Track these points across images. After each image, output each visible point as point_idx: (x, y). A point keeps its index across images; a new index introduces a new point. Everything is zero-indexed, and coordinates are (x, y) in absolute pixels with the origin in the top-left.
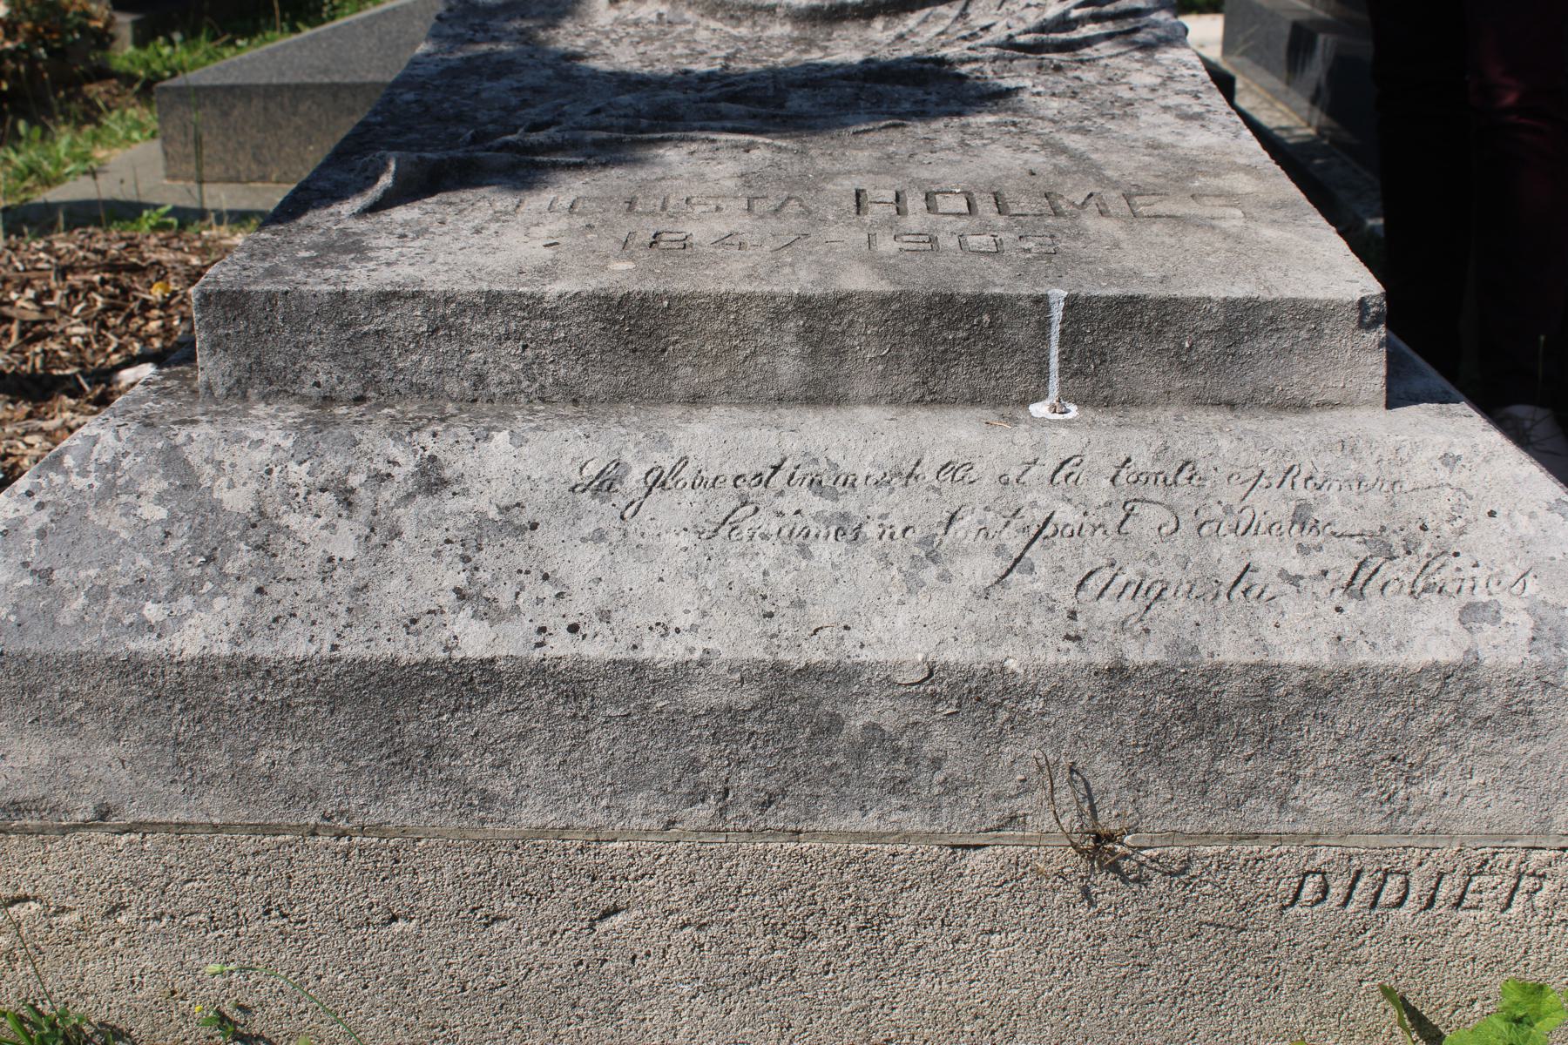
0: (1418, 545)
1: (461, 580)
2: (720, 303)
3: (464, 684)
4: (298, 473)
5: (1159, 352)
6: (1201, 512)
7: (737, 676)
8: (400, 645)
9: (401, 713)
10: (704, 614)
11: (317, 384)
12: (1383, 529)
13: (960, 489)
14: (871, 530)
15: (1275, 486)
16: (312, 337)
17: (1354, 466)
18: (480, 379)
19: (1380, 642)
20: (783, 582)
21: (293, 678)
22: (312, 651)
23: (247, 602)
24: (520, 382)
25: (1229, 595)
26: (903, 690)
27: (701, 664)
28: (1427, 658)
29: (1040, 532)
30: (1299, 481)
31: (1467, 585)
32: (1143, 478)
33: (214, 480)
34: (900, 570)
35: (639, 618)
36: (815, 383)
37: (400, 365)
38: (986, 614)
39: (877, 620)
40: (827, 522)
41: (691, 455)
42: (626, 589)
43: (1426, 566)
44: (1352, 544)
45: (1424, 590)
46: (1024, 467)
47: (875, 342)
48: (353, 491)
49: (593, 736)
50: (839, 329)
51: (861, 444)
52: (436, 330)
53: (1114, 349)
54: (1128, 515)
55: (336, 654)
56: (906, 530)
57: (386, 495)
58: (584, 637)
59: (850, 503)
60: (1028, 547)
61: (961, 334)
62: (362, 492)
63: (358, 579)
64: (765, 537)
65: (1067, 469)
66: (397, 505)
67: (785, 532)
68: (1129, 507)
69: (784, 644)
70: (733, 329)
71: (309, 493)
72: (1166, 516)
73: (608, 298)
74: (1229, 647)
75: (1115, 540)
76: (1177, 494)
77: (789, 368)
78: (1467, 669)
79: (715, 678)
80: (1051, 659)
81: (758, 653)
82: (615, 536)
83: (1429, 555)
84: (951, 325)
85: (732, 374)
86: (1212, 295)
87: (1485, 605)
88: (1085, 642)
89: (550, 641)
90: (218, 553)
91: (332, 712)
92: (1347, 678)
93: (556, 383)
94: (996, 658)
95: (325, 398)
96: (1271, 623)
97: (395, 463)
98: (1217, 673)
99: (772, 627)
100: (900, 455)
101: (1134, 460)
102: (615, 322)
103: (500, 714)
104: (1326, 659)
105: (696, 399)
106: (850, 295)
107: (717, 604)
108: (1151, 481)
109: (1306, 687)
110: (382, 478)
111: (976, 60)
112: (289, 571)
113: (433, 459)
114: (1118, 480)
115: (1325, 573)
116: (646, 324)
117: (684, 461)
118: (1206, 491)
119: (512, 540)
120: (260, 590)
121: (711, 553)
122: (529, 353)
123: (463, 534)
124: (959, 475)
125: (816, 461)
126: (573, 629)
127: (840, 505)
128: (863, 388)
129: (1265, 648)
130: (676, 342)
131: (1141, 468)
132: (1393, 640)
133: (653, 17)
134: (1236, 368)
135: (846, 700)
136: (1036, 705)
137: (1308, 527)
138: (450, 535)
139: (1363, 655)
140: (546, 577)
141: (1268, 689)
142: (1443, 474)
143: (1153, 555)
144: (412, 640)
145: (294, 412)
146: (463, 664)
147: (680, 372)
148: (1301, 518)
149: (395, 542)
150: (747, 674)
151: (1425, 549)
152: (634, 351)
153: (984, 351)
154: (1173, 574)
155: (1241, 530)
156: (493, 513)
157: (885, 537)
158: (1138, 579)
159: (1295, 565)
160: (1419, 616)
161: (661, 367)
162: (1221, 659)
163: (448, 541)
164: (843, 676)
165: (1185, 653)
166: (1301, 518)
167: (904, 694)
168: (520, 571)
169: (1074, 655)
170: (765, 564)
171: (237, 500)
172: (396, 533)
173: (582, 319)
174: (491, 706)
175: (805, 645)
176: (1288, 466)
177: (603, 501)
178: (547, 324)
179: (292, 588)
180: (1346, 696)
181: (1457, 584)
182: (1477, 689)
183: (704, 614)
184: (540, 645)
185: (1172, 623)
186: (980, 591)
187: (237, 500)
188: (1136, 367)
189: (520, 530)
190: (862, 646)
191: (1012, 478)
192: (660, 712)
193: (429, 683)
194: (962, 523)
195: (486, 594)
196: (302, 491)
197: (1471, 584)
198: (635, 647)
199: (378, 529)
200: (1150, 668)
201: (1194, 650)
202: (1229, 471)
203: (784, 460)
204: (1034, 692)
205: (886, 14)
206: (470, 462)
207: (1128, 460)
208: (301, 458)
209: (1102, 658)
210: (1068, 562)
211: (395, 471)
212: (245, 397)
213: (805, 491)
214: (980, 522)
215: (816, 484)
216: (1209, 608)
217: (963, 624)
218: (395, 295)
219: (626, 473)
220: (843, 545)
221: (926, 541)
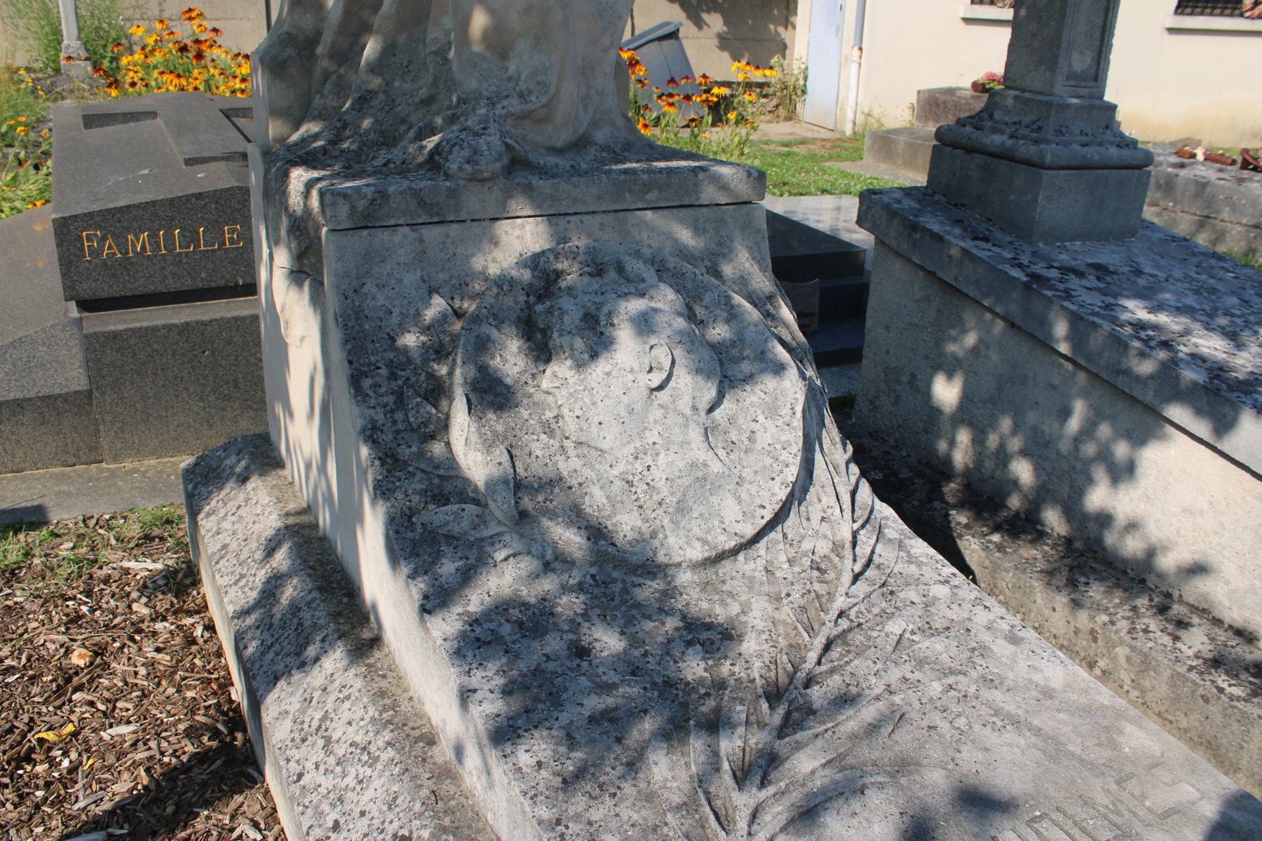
133: (589, 579)
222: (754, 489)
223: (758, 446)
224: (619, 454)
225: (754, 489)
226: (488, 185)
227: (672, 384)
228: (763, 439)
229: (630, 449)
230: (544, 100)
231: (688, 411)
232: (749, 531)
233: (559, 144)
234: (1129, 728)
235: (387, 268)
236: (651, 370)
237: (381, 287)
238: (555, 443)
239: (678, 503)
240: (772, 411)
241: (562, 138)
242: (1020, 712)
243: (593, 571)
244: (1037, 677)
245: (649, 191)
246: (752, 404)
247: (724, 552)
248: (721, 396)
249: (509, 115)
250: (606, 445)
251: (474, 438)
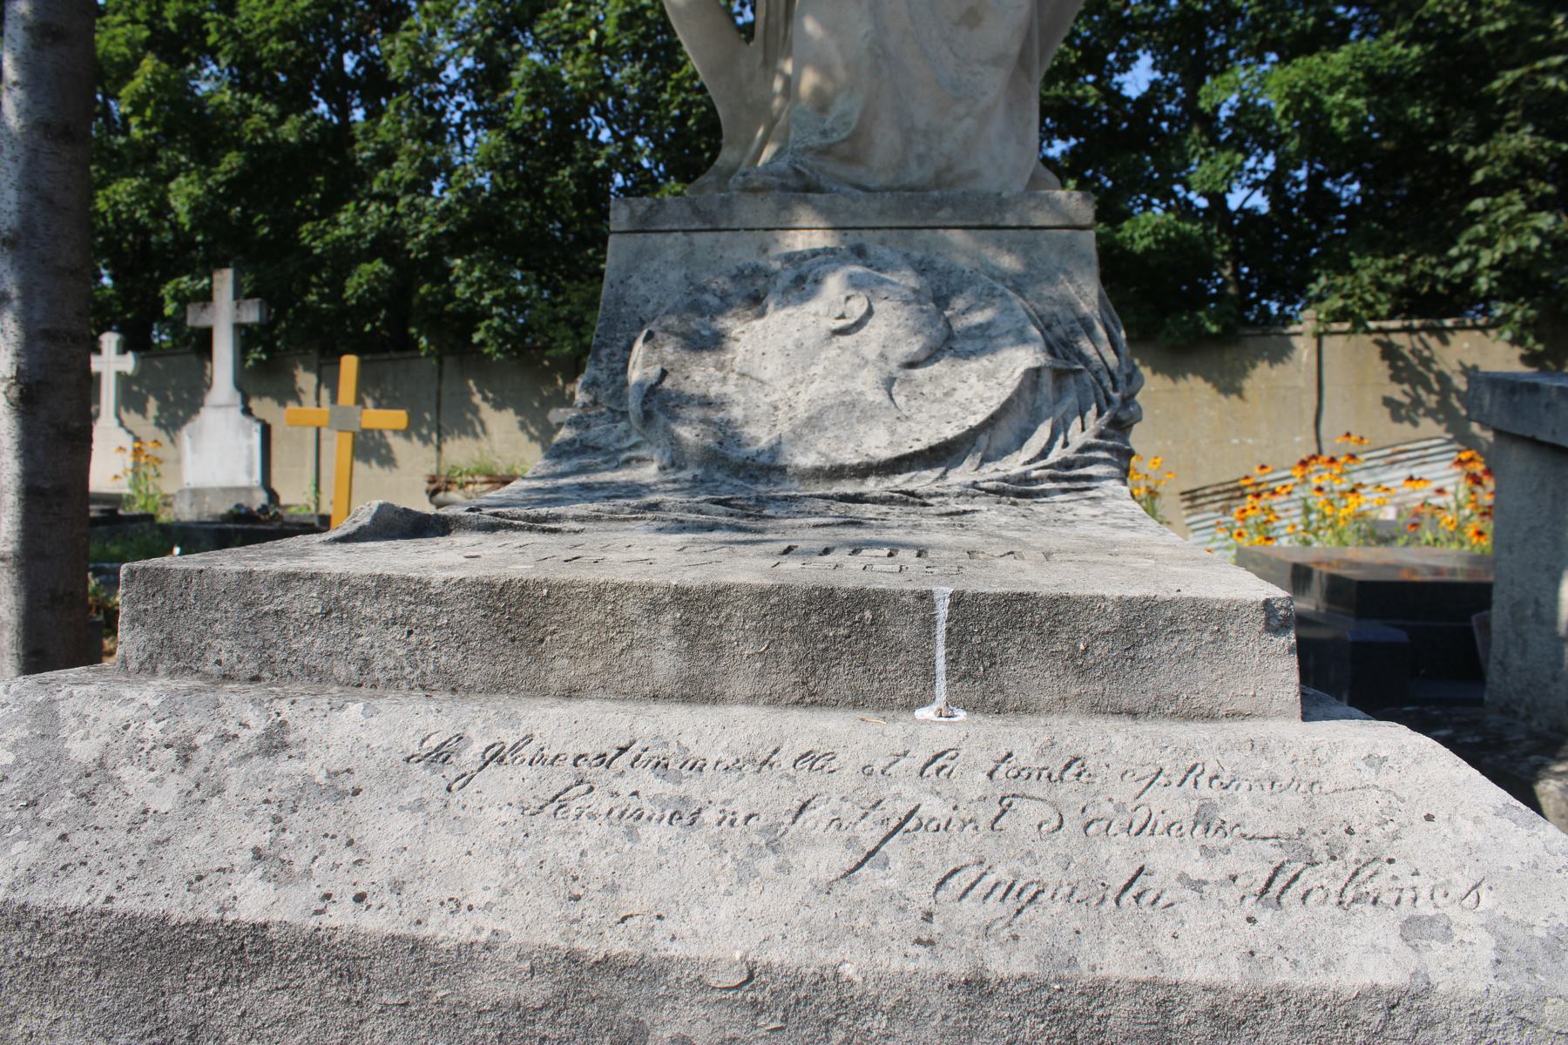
0: (1345, 849)
1: (261, 838)
2: (598, 593)
3: (234, 952)
5: (1053, 654)
6: (1088, 810)
7: (527, 965)
8: (175, 902)
9: (167, 982)
10: (504, 892)
11: (219, 662)
12: (1302, 832)
13: (816, 778)
14: (710, 816)
15: (1175, 784)
16: (218, 615)
17: (1265, 765)
18: (366, 662)
19: (1303, 959)
20: (600, 864)
21: (62, 932)
22: (85, 902)
23: (45, 848)
24: (402, 668)
25: (1117, 901)
26: (717, 995)
27: (488, 948)
28: (1364, 980)
29: (901, 825)
30: (1203, 780)
31: (1407, 896)
32: (1025, 774)
33: (72, 731)
34: (733, 858)
35: (433, 892)
36: (691, 680)
37: (294, 646)
38: (823, 911)
39: (696, 911)
40: (664, 805)
41: (537, 733)
42: (429, 861)
43: (1356, 874)
44: (1266, 847)
45: (1354, 901)
46: (892, 759)
47: (753, 637)
48: (195, 748)
49: (367, 1027)
50: (717, 623)
51: (718, 730)
52: (329, 613)
53: (1005, 650)
54: (1004, 811)
55: (109, 906)
56: (750, 817)
57: (225, 754)
58: (368, 907)
59: (693, 788)
60: (885, 840)
61: (842, 631)
62: (204, 750)
64: (592, 816)
65: (940, 762)
66: (231, 765)
67: (616, 813)
68: (1006, 802)
69: (584, 931)
70: (610, 620)
71: (154, 748)
72: (1048, 812)
73: (491, 585)
74: (1115, 960)
75: (986, 836)
76: (1062, 790)
77: (665, 663)
78: (1414, 997)
79: (502, 965)
80: (896, 965)
81: (553, 939)
82: (435, 807)
83: (1357, 861)
84: (832, 622)
85: (607, 667)
86: (1107, 594)
87: (1432, 920)
88: (939, 947)
89: (332, 909)
90: (42, 800)
91: (97, 975)
92: (1264, 1003)
93: (437, 671)
94: (829, 960)
95: (224, 676)
96: (1168, 932)
97: (244, 725)
98: (1099, 991)
99: (576, 910)
100: (758, 742)
101: (1015, 754)
102: (496, 610)
103: (270, 992)
104: (1236, 978)
105: (571, 693)
106: (728, 588)
107: (521, 883)
108: (1034, 777)
109: (1213, 1013)
110: (226, 738)
111: (942, 495)
112: (101, 820)
113: (283, 724)
114: (996, 774)
115: (1234, 878)
116: (526, 612)
117: (529, 739)
118: (1096, 787)
119: (330, 804)
120: (64, 837)
121: (531, 829)
122: (413, 638)
123: (284, 795)
124: (817, 765)
125: (666, 744)
126: (360, 898)
127: (682, 789)
128: (740, 685)
129: (1159, 962)
130: (554, 632)
131: (1023, 764)
132: (1319, 958)
134: (1136, 673)
135: (651, 1004)
136: (878, 1023)
137: (1213, 828)
138: (270, 796)
139: (1281, 975)
140: (350, 843)
141: (1166, 1015)
142: (1368, 775)
143: (1029, 853)
144: (191, 896)
145: (185, 683)
146: (233, 928)
147: (558, 663)
148: (1205, 819)
149: (215, 799)
150: (538, 964)
151: (1353, 854)
152: (513, 640)
153: (866, 649)
154: (1051, 874)
155: (1133, 831)
156: (321, 777)
157: (725, 823)
158: (1010, 880)
159: (1198, 868)
160: (1351, 930)
161: (538, 657)
162: (1104, 973)
163: (267, 801)
164: (646, 972)
165: (1060, 965)
166: (1205, 819)
167: (720, 1001)
168: (326, 835)
169: (924, 962)
170: (585, 843)
172: (218, 791)
173: (465, 605)
174: (260, 982)
175: (607, 934)
176: (1190, 764)
178: (431, 610)
179: (95, 836)
180: (1264, 1028)
181: (1396, 894)
182: (1432, 1024)
183: (504, 892)
184: (318, 912)
185: (1048, 929)
186: (823, 886)
187: (82, 750)
188: (1027, 671)
189: (342, 795)
190: (674, 938)
192: (440, 1003)
193: (198, 947)
194: (813, 812)
195: (283, 856)
197: (1412, 894)
198: (419, 922)
199: (203, 785)
200: (1017, 982)
201: (1072, 962)
202: (1123, 768)
203: (634, 742)
204: (874, 1007)
205: (878, 475)
206: (317, 727)
207: (1010, 755)
208: (161, 716)
209: (958, 968)
210: (930, 857)
211: (245, 734)
212: (154, 672)
213: (647, 774)
214: (833, 813)
215: (661, 766)
216: (1093, 914)
217: (796, 920)
218: (295, 575)
219: (466, 746)
220: (677, 827)
221: (771, 829)
222: (916, 428)
223: (951, 400)
224: (777, 384)
225: (916, 428)
226: (760, 195)
227: (863, 332)
228: (963, 394)
229: (790, 380)
230: (844, 135)
231: (872, 356)
232: (886, 454)
233: (872, 186)
235: (655, 264)
236: (842, 317)
237: (645, 280)
238: (720, 375)
239: (810, 418)
240: (989, 375)
241: (881, 180)
243: (699, 472)
245: (940, 208)
246: (970, 370)
247: (842, 467)
248: (931, 357)
249: (808, 149)
250: (765, 376)
251: (640, 360)
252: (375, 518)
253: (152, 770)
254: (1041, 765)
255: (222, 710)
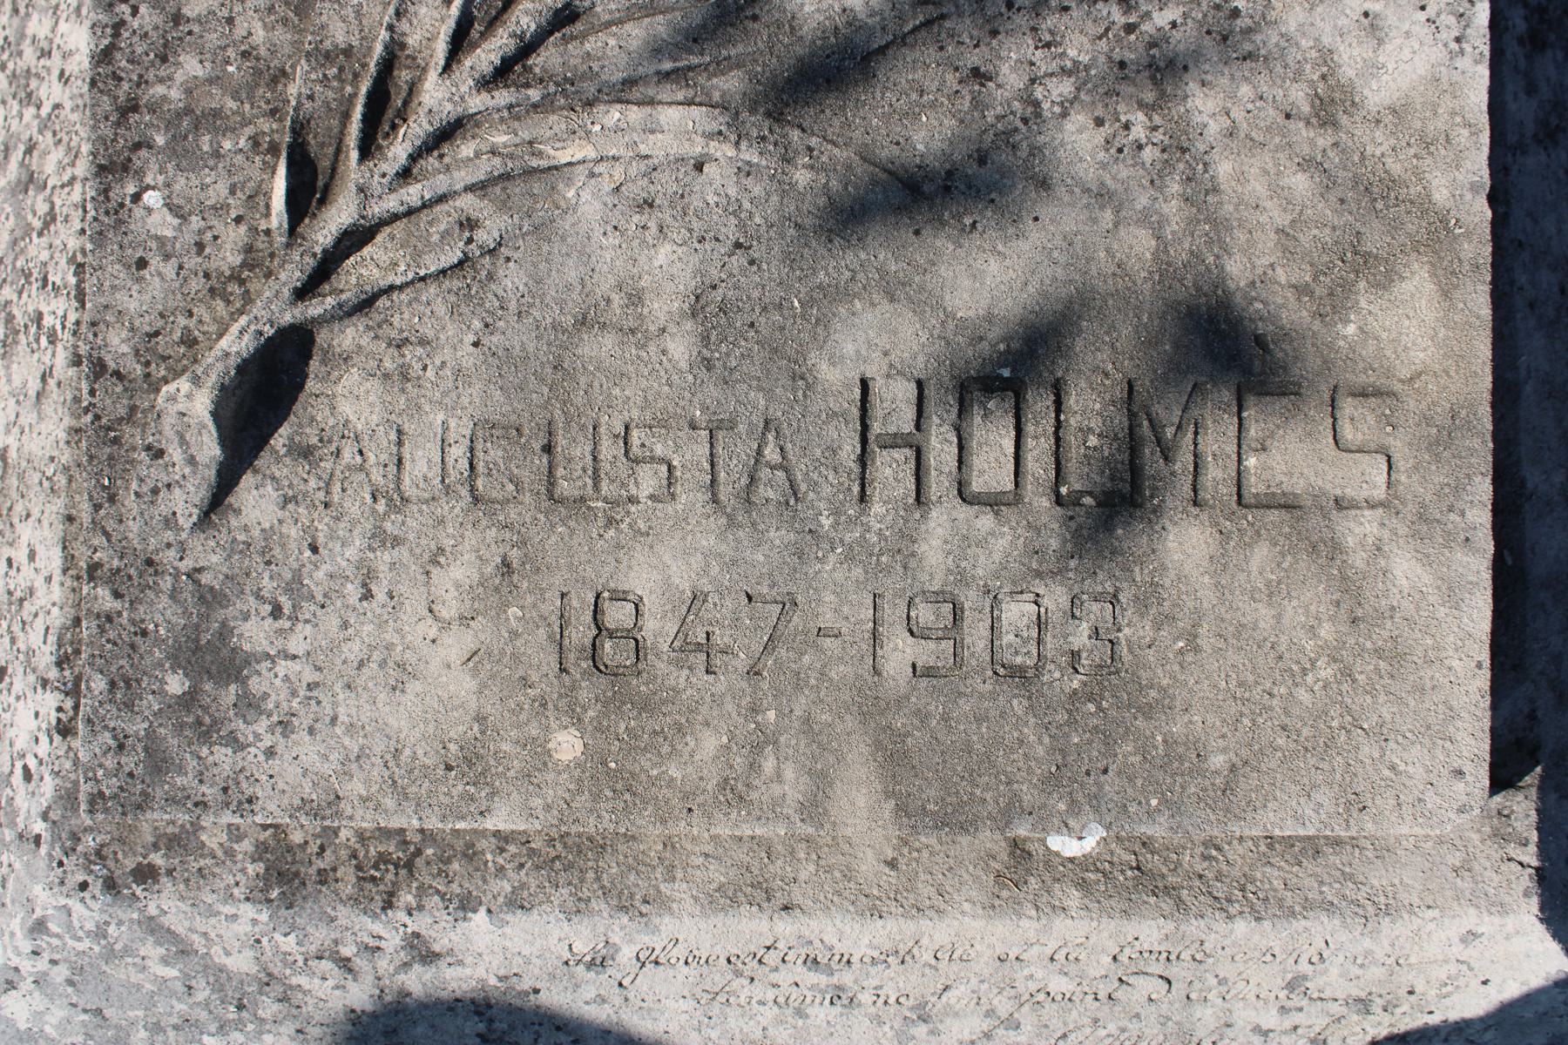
4: (289, 943)
14: (866, 998)
48: (349, 960)
59: (846, 978)
63: (385, 1025)
64: (762, 1003)
66: (397, 972)
67: (781, 1000)
97: (380, 938)
115: (1296, 1028)
151: (1398, 1011)
159: (1270, 1019)
171: (241, 963)
177: (597, 973)
191: (1012, 956)
196: (300, 959)
206: (454, 938)
210: (1054, 1021)
211: (383, 944)
215: (813, 963)
220: (838, 1009)
221: (922, 1006)
234: (1417, 283)
242: (1213, 128)
244: (1351, 57)
252: (223, 441)
253: (324, 979)
254: (1162, 949)
255: (342, 922)
